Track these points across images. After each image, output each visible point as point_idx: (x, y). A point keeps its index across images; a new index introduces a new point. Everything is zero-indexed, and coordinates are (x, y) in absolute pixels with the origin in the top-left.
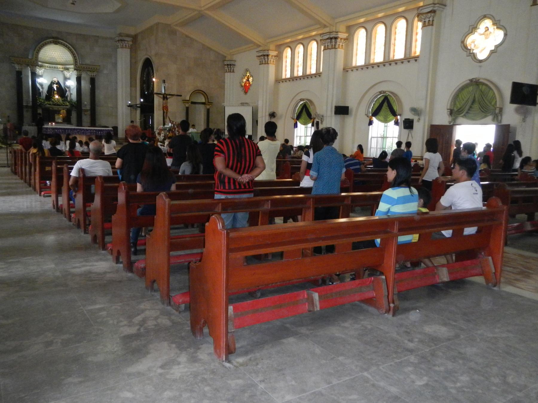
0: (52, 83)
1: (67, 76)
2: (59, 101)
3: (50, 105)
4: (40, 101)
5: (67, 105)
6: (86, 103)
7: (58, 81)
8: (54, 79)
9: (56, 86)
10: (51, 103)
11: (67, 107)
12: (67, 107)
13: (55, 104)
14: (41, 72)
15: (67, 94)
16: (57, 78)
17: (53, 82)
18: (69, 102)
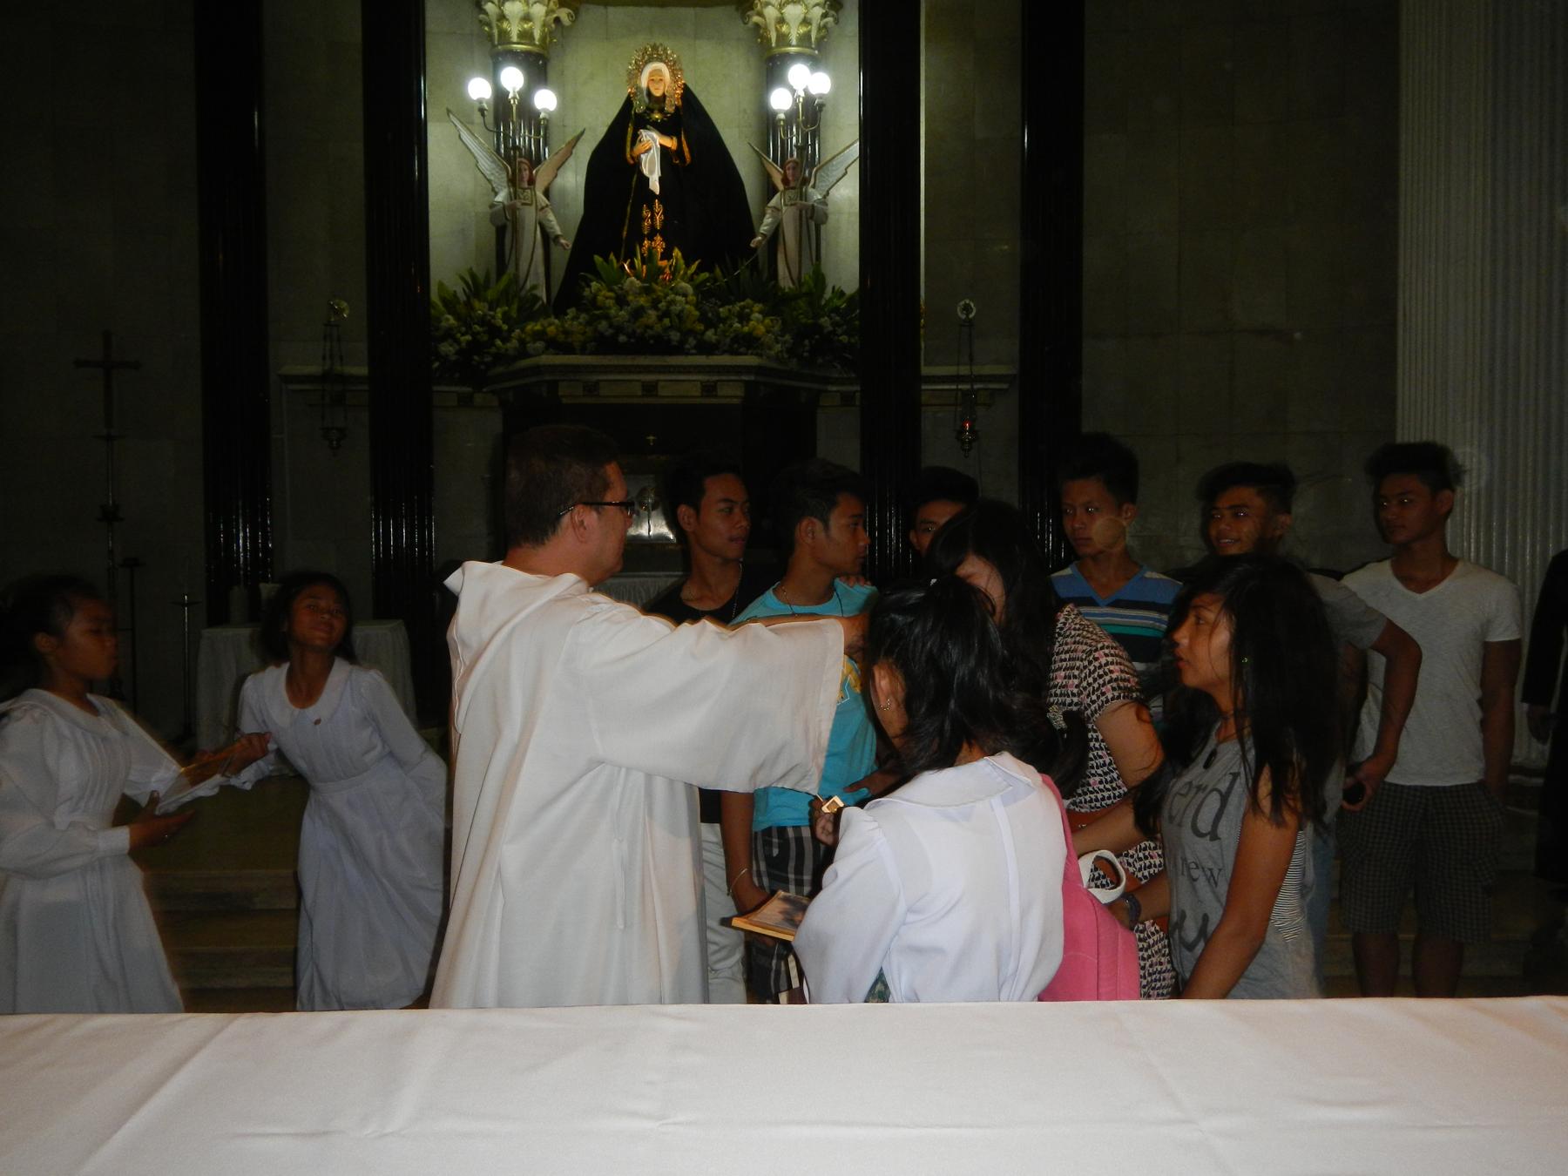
0: (628, 121)
1: (783, 39)
2: (655, 304)
3: (554, 345)
4: (466, 321)
5: (749, 342)
6: (966, 307)
7: (688, 96)
8: (644, 82)
9: (664, 149)
10: (574, 321)
11: (750, 360)
12: (750, 360)
13: (619, 329)
14: (527, 18)
15: (764, 229)
16: (675, 69)
17: (639, 107)
18: (776, 303)
